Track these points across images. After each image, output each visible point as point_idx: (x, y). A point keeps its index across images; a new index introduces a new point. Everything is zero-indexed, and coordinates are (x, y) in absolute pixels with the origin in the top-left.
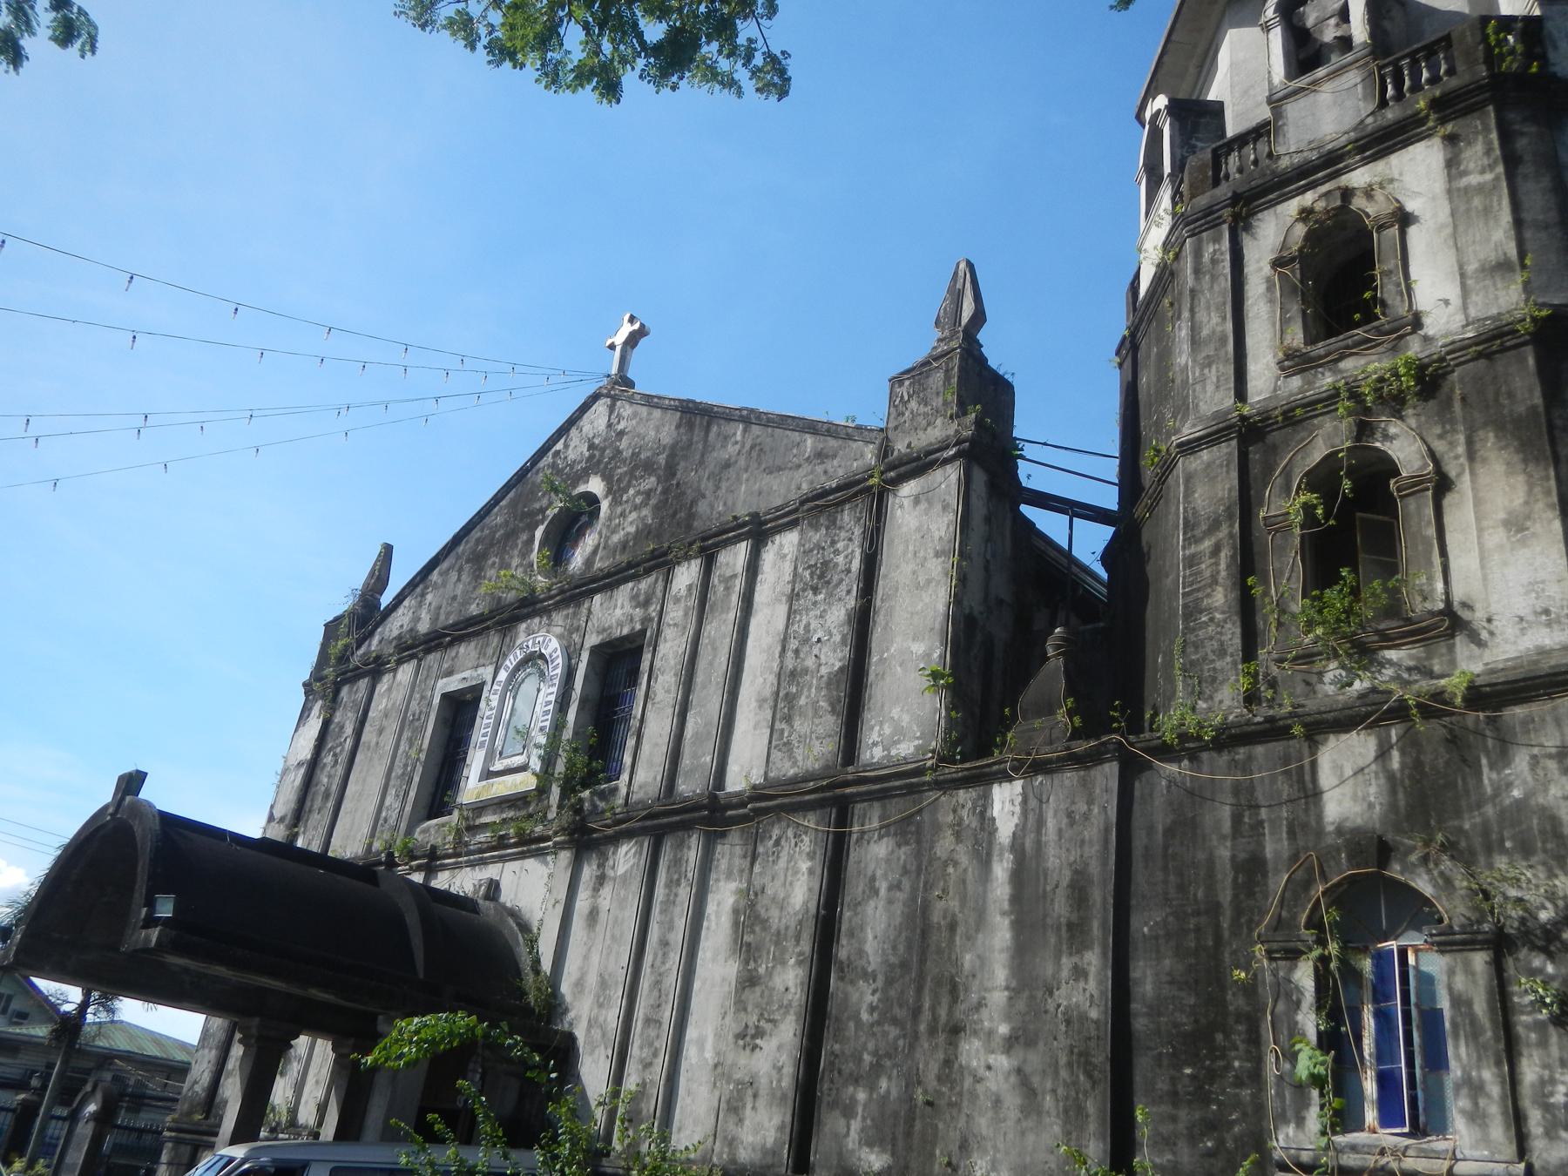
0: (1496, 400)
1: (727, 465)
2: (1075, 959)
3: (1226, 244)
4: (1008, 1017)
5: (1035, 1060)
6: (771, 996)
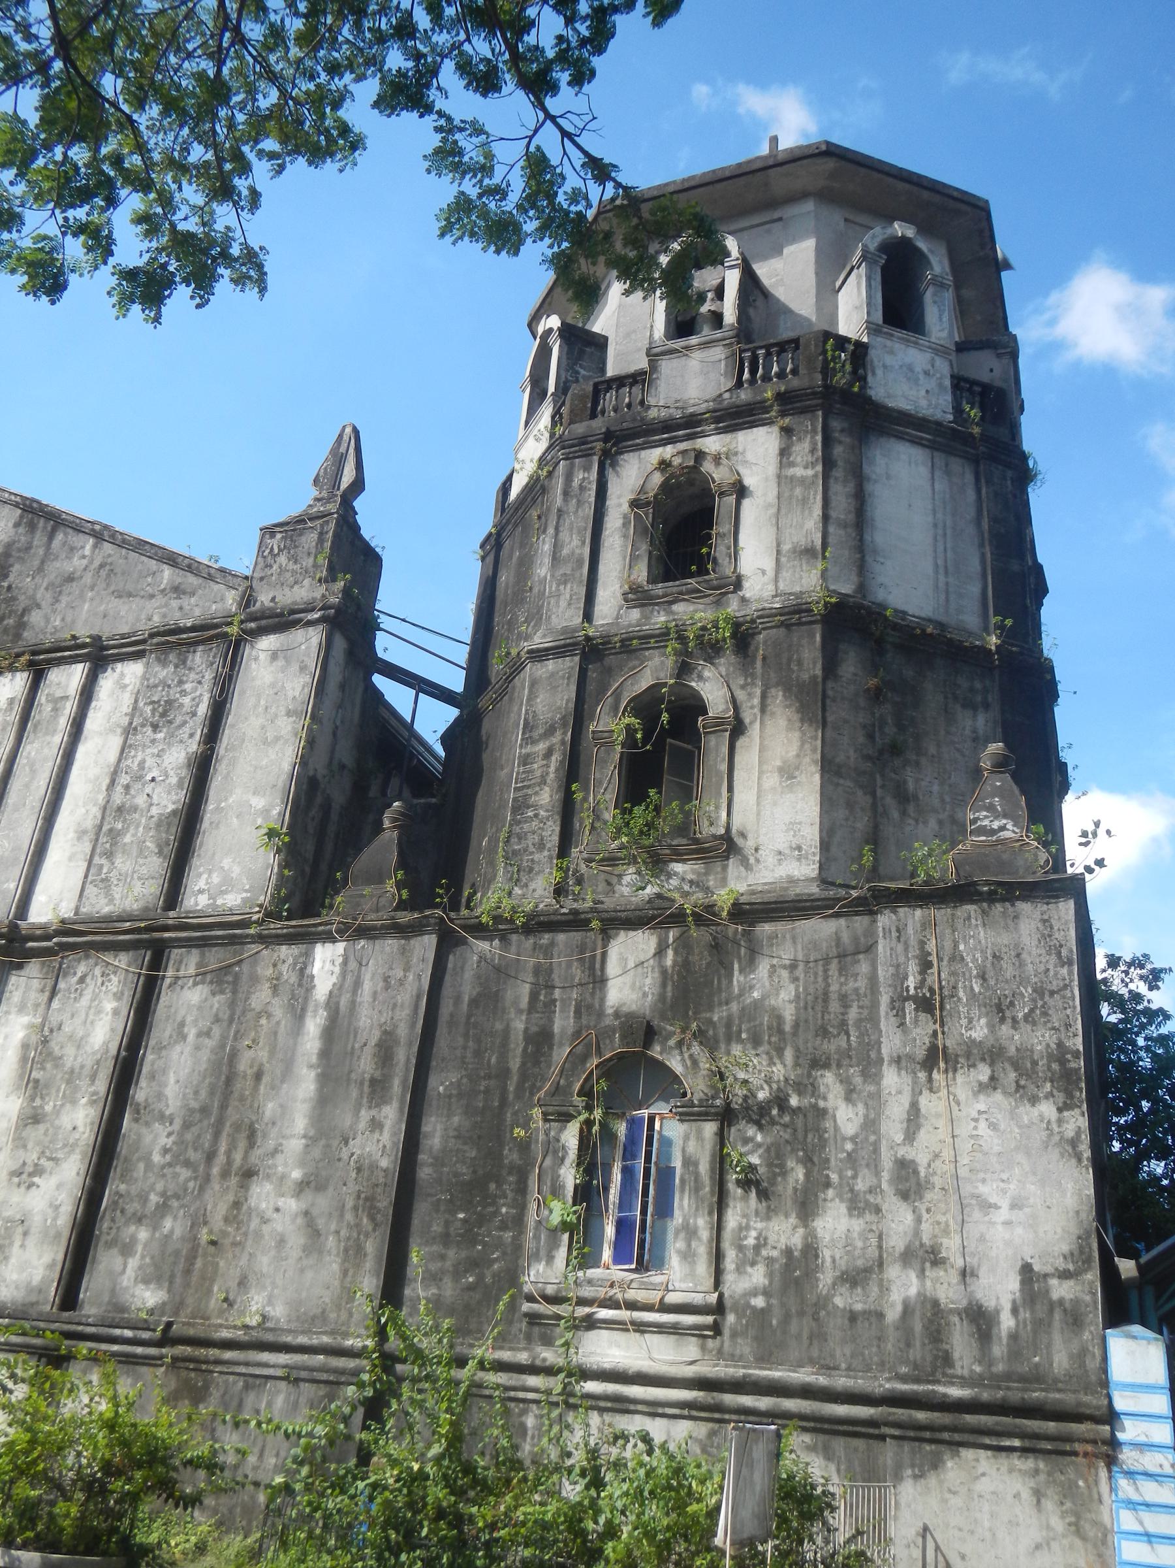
0: (789, 665)
1: (70, 579)
2: (374, 1112)
4: (302, 1163)
5: (323, 1203)
6: (56, 1134)
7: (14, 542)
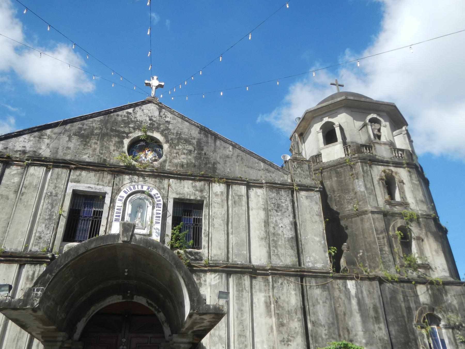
1: (228, 157)
2: (378, 325)
3: (369, 169)
4: (365, 338)
6: (290, 329)
7: (201, 139)
